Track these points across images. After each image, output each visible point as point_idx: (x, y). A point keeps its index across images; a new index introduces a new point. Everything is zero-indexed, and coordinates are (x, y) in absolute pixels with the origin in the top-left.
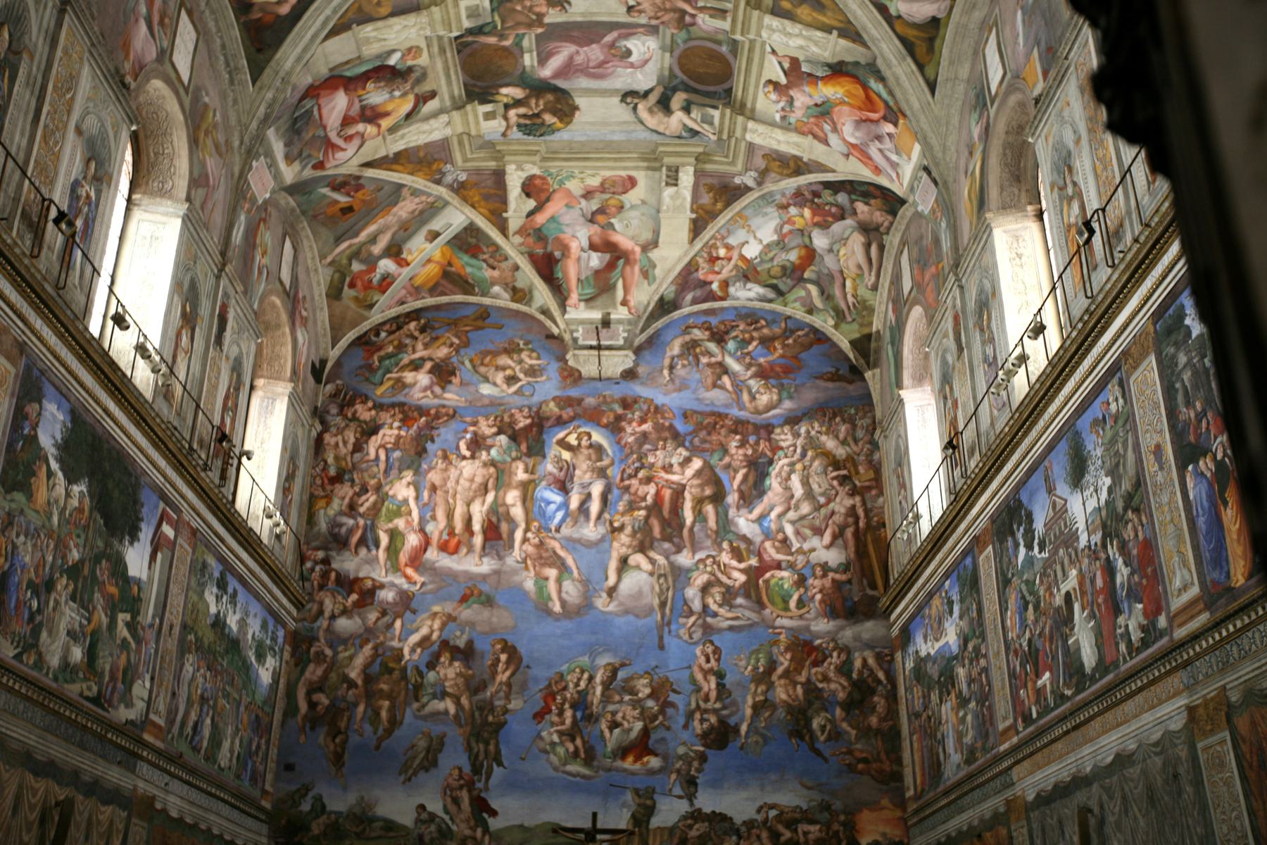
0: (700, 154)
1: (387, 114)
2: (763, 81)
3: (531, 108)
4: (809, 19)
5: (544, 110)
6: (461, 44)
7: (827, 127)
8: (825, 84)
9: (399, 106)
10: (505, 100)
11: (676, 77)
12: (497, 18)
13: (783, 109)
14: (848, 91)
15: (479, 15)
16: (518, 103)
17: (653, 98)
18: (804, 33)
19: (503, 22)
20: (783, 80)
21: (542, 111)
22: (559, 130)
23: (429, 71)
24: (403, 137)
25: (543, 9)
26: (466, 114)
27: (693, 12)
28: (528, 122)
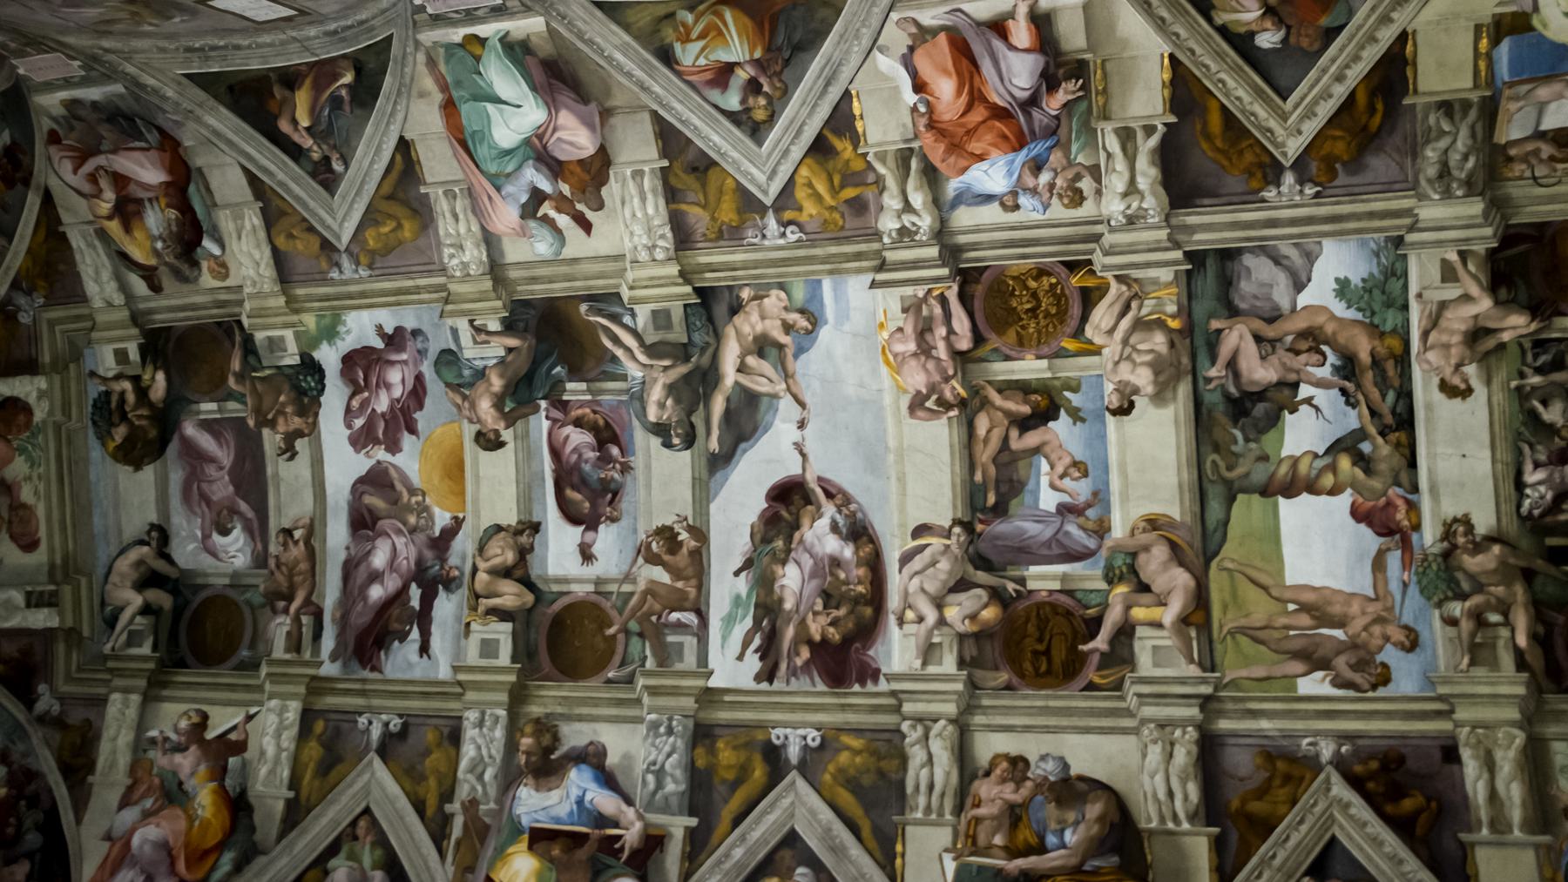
0: (80, 634)
1: (127, 229)
2: (205, 708)
4: (305, 757)
5: (133, 429)
6: (231, 328)
7: (148, 803)
8: (215, 792)
9: (139, 246)
10: (147, 377)
11: (195, 593)
12: (268, 372)
13: (166, 739)
14: (209, 822)
15: (272, 351)
17: (160, 565)
18: (284, 754)
20: (210, 735)
22: (104, 445)
23: (191, 287)
24: (91, 246)
25: (281, 428)
26: (123, 327)
27: (293, 608)
28: (114, 404)
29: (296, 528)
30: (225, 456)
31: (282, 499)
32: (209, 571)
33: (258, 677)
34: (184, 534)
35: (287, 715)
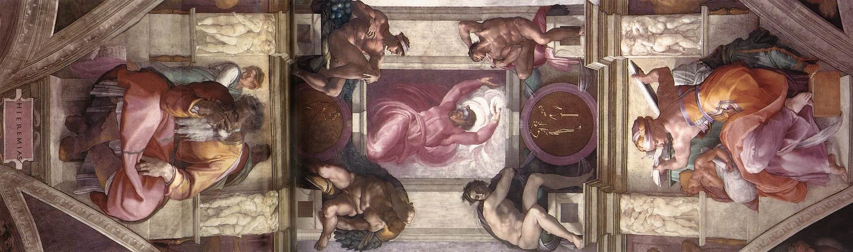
3: (356, 210)
7: (721, 166)
8: (706, 94)
12: (327, 51)
13: (661, 161)
14: (735, 91)
16: (339, 195)
17: (502, 191)
18: (669, 26)
19: (333, 59)
20: (655, 113)
21: (368, 210)
22: (387, 240)
25: (378, 47)
27: (540, 41)
28: (349, 228)
29: (469, 39)
30: (402, 114)
31: (443, 55)
32: (507, 137)
33: (603, 68)
34: (473, 165)
35: (635, 33)
